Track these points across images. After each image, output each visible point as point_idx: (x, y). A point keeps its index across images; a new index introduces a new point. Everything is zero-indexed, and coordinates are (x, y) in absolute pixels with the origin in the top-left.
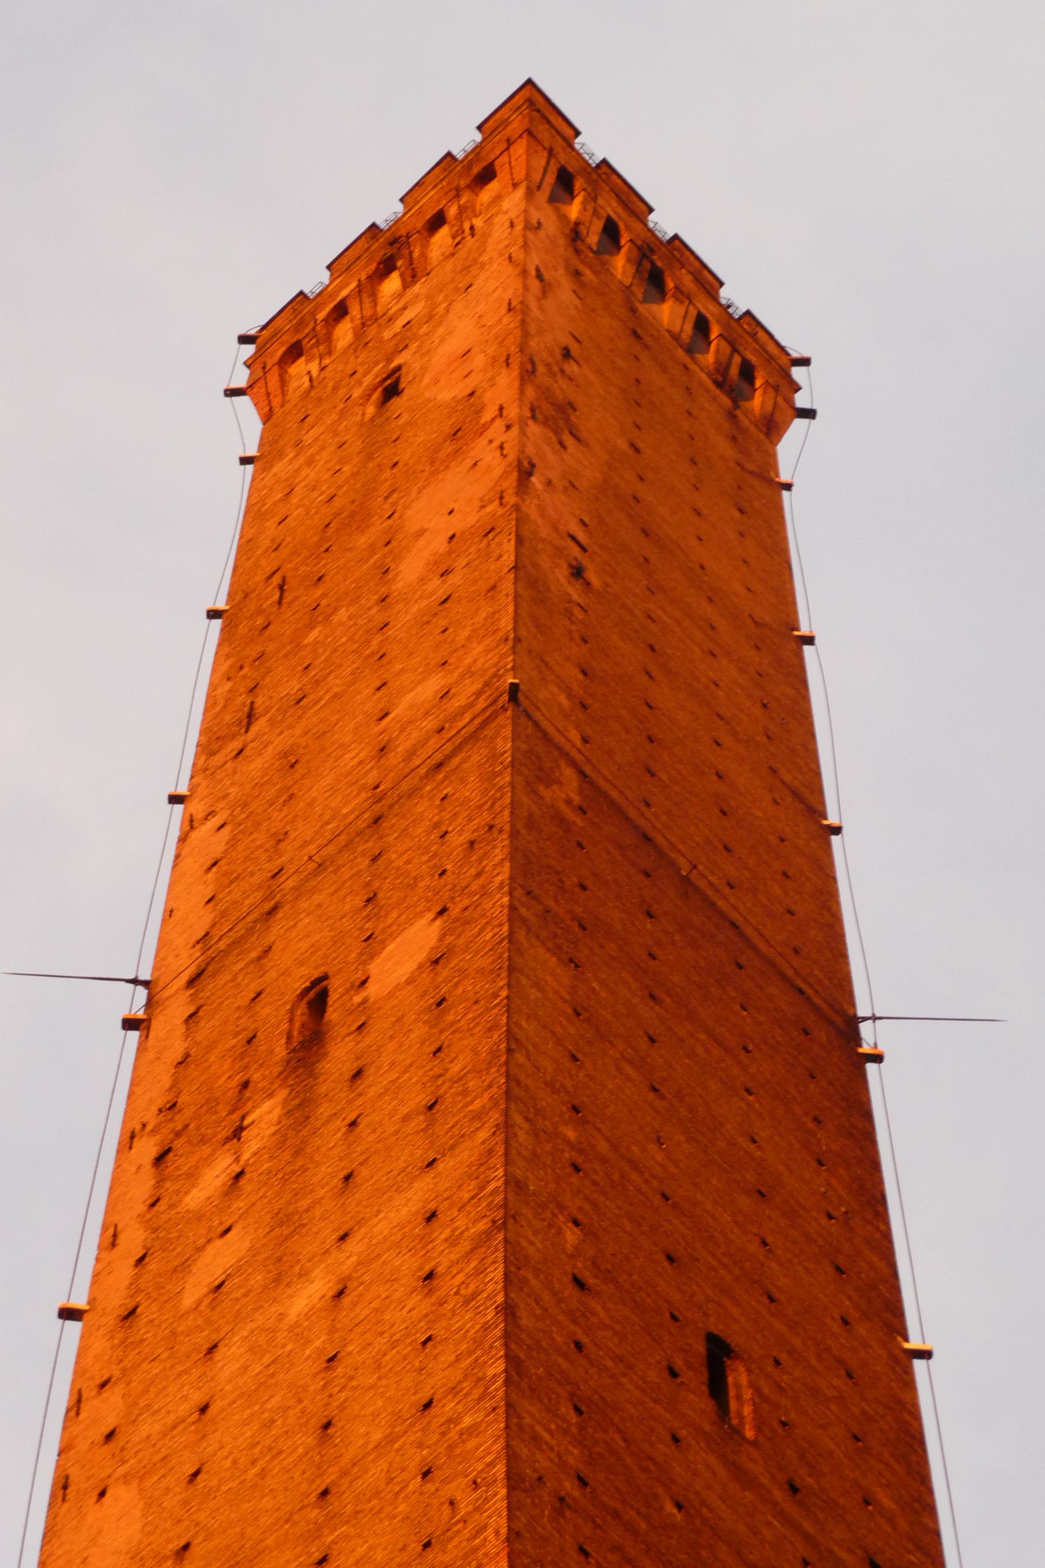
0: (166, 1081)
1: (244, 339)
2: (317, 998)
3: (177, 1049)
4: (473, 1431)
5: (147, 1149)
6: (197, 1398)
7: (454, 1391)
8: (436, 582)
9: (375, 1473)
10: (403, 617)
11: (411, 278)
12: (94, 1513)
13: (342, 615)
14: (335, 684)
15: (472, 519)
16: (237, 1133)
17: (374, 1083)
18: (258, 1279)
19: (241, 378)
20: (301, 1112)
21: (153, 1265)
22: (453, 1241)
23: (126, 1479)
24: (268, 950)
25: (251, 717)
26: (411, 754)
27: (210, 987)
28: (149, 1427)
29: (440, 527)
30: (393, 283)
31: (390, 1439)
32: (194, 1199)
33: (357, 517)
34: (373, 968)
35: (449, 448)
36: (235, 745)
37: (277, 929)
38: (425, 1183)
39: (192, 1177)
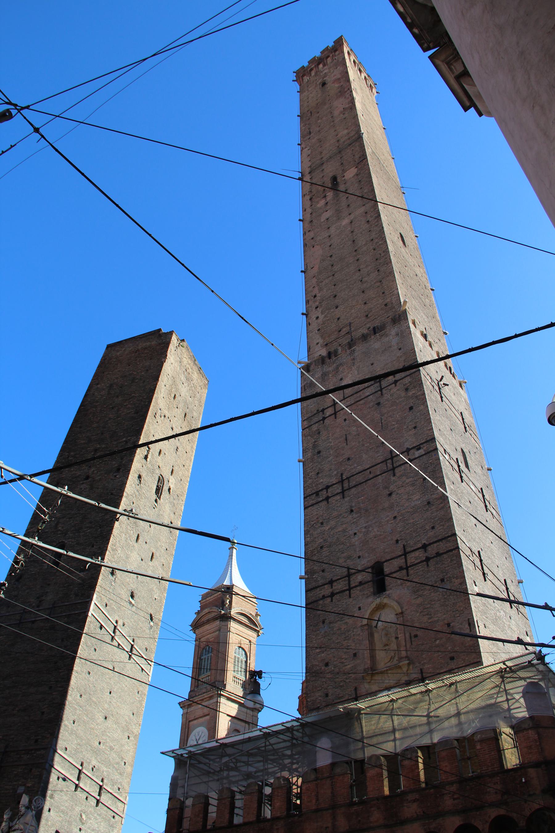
1: (294, 72)
2: (334, 179)
4: (382, 244)
5: (308, 197)
6: (328, 234)
7: (377, 238)
8: (342, 115)
9: (365, 248)
11: (324, 65)
13: (324, 118)
15: (347, 106)
16: (325, 196)
18: (335, 218)
19: (295, 79)
21: (314, 214)
22: (371, 217)
23: (317, 245)
24: (323, 170)
25: (310, 133)
26: (344, 142)
28: (319, 238)
30: (321, 66)
31: (366, 244)
32: (319, 206)
34: (345, 174)
35: (339, 94)
36: (308, 137)
37: (324, 167)
39: (318, 202)
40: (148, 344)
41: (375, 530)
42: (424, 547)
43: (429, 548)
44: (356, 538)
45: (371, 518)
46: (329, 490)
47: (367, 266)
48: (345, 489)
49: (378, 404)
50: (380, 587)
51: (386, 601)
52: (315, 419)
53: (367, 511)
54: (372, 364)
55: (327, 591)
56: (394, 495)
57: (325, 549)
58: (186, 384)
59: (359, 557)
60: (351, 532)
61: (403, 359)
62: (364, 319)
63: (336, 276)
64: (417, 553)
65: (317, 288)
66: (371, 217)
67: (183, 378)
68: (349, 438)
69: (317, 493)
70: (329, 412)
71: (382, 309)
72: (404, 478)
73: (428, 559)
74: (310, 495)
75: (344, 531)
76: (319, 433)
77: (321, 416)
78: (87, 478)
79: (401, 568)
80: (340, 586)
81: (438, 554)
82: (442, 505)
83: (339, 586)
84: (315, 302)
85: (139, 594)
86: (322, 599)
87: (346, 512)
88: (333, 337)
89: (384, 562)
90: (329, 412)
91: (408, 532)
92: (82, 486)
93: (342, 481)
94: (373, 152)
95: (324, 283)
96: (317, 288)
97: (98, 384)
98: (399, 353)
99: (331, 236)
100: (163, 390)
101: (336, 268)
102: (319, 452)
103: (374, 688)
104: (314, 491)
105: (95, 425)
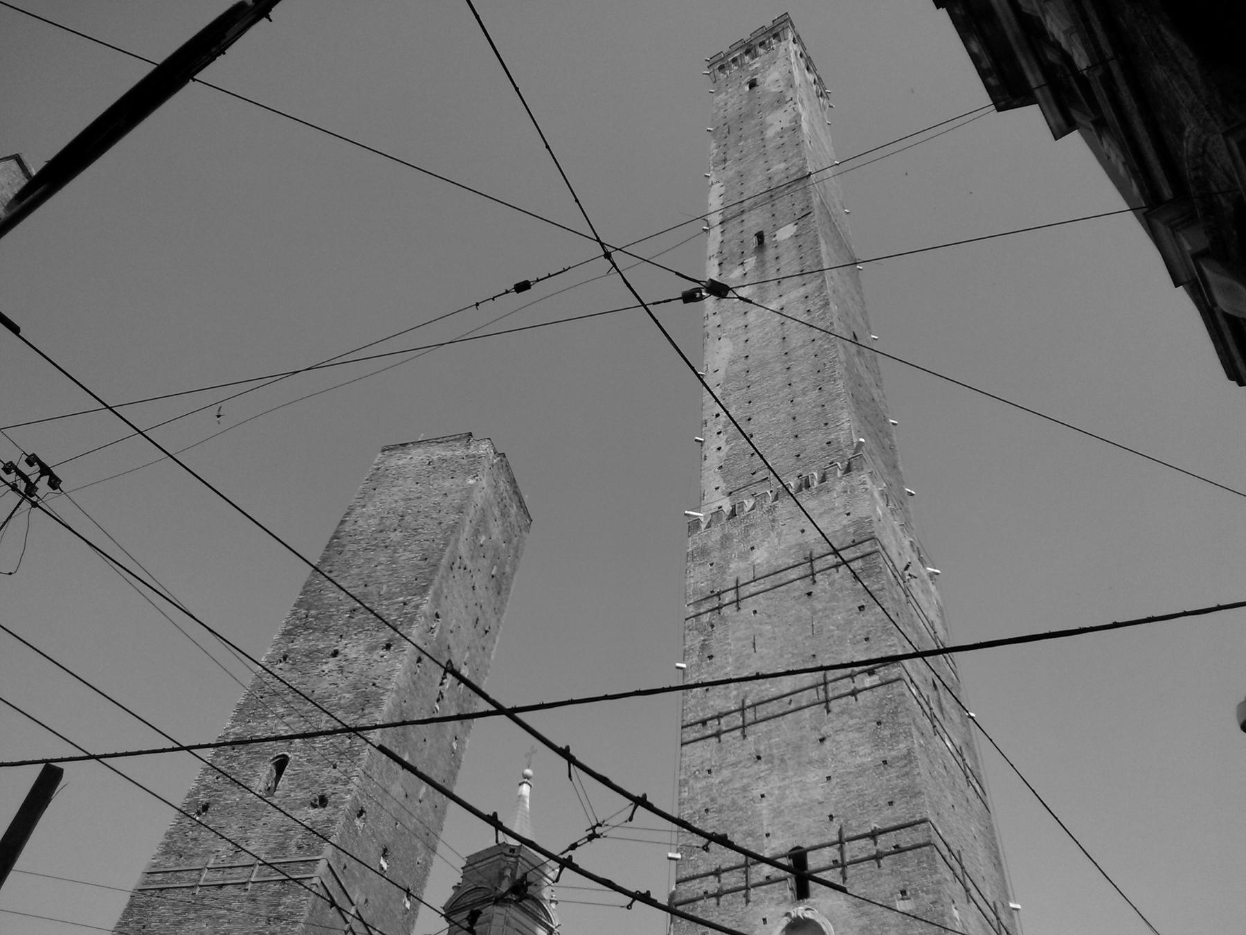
0: (718, 245)
2: (760, 236)
3: (720, 239)
9: (802, 352)
10: (770, 146)
12: (718, 342)
14: (751, 157)
17: (783, 262)
20: (761, 264)
25: (725, 160)
27: (727, 226)
29: (777, 128)
33: (750, 115)
37: (744, 217)
39: (731, 271)
40: (449, 454)
41: (796, 794)
42: (873, 835)
43: (881, 838)
44: (764, 804)
45: (790, 773)
46: (722, 721)
47: (803, 379)
48: (747, 721)
49: (809, 594)
51: (809, 915)
52: (707, 606)
53: (782, 761)
54: (803, 531)
55: (711, 885)
56: (827, 743)
57: (711, 815)
58: (499, 522)
59: (768, 835)
60: (757, 793)
61: (851, 530)
62: (793, 460)
63: (752, 389)
64: (863, 842)
66: (814, 304)
67: (497, 512)
68: (759, 641)
69: (704, 722)
70: (729, 597)
71: (822, 449)
72: (845, 717)
73: (878, 857)
74: (692, 725)
75: (745, 789)
76: (712, 626)
77: (715, 603)
78: (335, 654)
80: (734, 880)
81: (898, 849)
82: (907, 769)
83: (731, 880)
84: (716, 424)
85: (395, 853)
86: (702, 898)
87: (749, 759)
88: (742, 482)
89: (809, 850)
90: (729, 597)
91: (848, 804)
92: (324, 667)
93: (742, 710)
94: (822, 203)
95: (732, 398)
97: (364, 506)
98: (845, 521)
100: (467, 529)
101: (753, 377)
102: (711, 657)
104: (698, 719)
105: (355, 571)
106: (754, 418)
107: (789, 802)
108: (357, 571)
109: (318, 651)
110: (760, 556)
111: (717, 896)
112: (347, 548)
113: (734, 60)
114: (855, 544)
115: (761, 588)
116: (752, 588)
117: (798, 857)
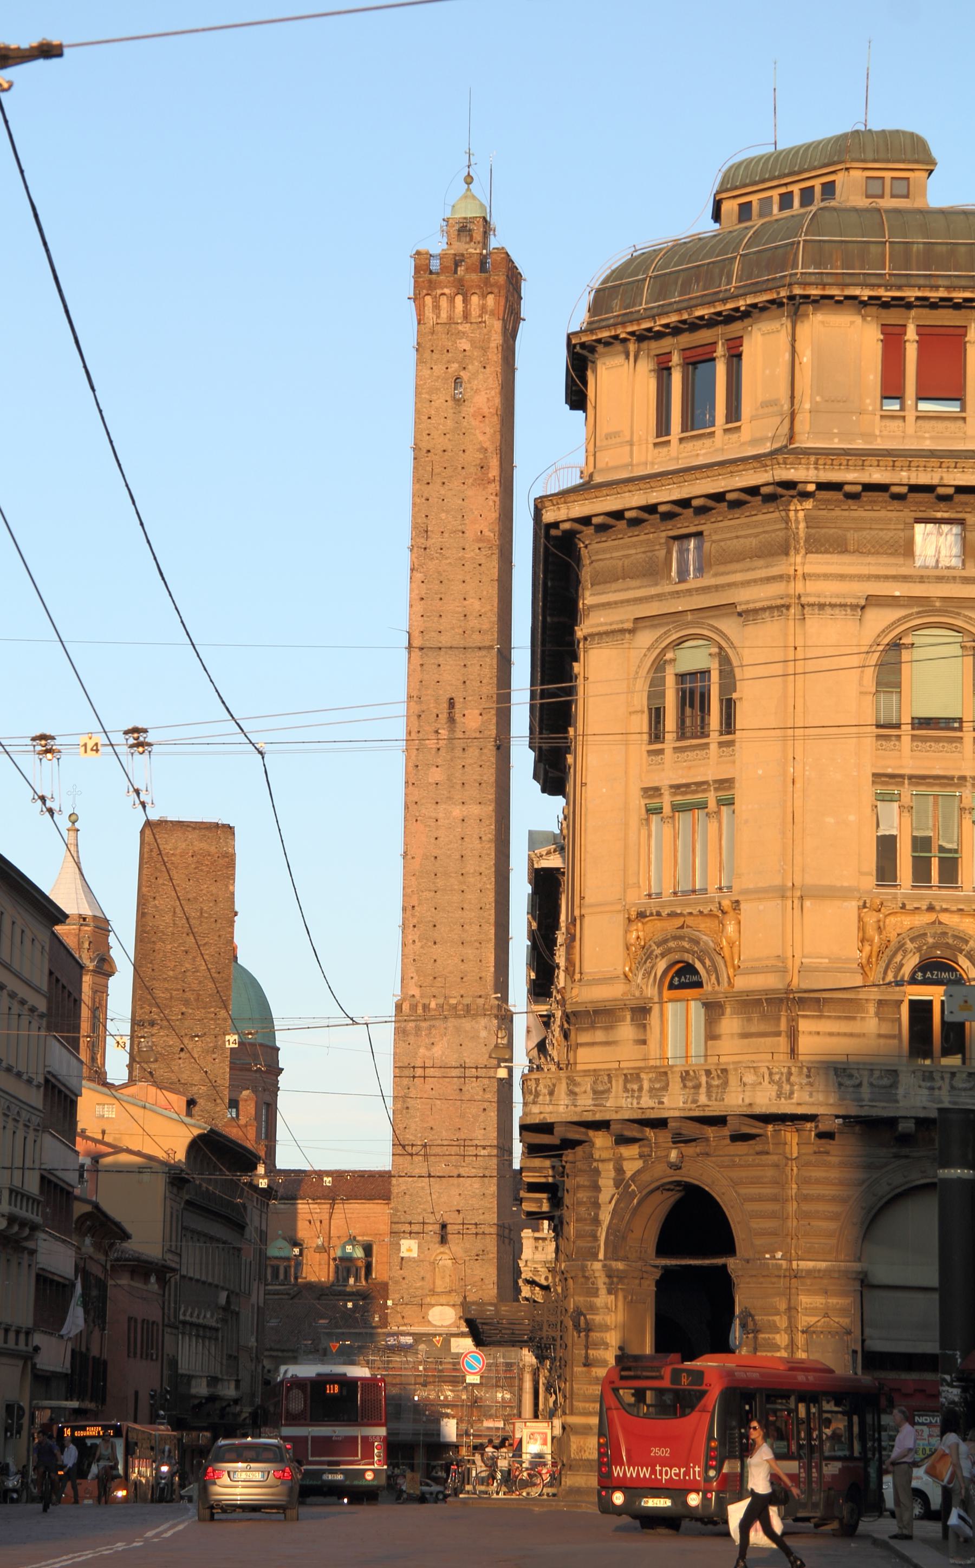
2: (451, 703)
6: (434, 815)
21: (421, 757)
38: (479, 807)
50: (443, 1240)
55: (407, 1228)
62: (459, 980)
65: (415, 897)
70: (419, 1072)
73: (477, 1234)
79: (459, 1233)
81: (484, 1233)
83: (415, 1228)
90: (419, 1072)
96: (415, 897)
99: (439, 823)
101: (440, 883)
103: (433, 1302)
106: (438, 926)
107: (442, 1200)
108: (171, 973)
109: (170, 1046)
110: (437, 1051)
111: (410, 1233)
112: (157, 947)
113: (443, 294)
114: (486, 1067)
115: (437, 1074)
116: (430, 1072)
117: (444, 1226)
